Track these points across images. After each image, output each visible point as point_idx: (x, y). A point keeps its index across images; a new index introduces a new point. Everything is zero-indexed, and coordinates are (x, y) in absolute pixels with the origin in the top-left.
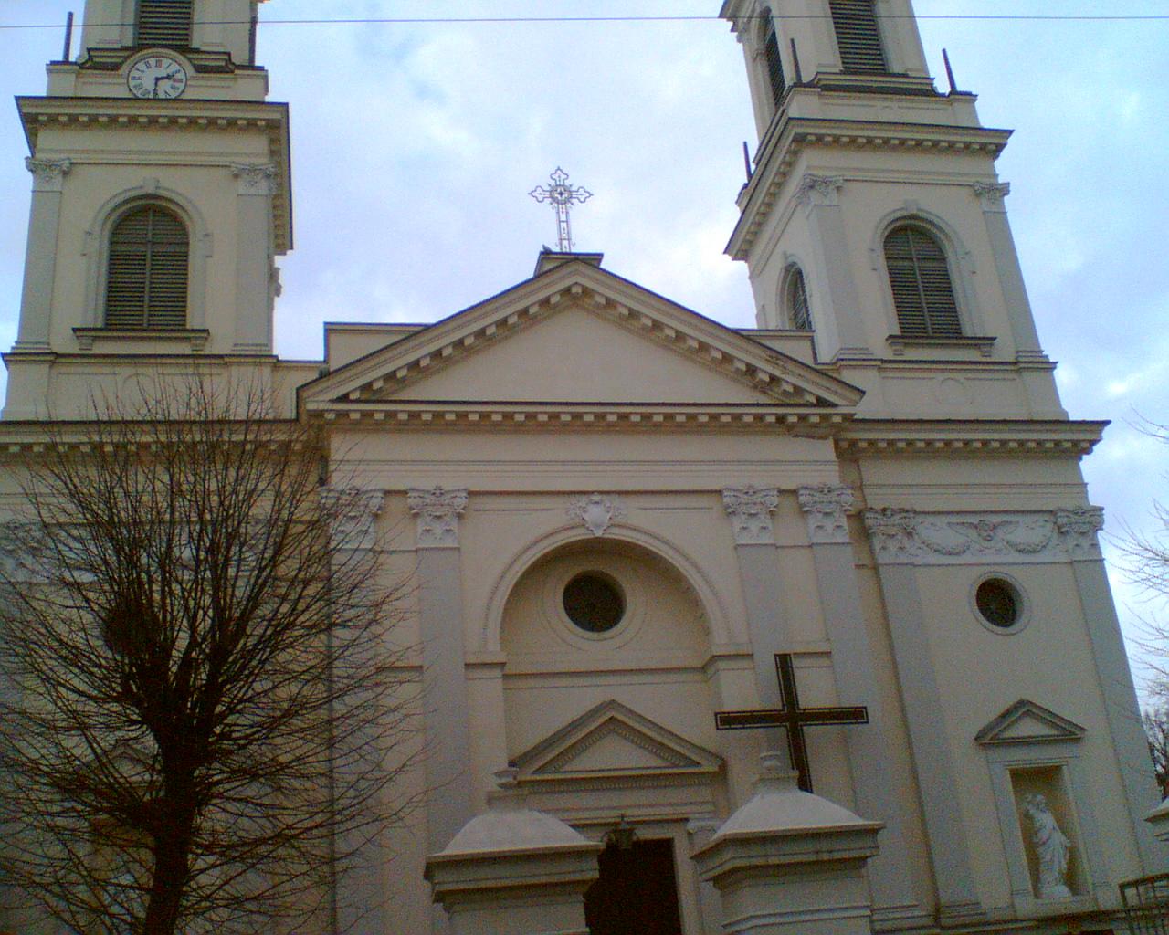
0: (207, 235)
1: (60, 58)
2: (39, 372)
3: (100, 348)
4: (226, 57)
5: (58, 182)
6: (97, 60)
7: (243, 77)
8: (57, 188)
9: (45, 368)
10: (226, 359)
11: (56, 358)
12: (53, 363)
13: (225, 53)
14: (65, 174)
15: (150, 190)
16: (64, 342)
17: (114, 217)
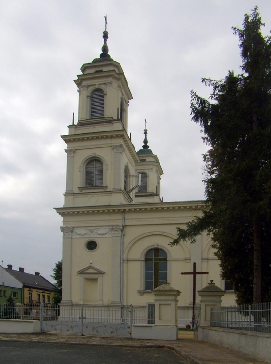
0: (106, 165)
1: (72, 124)
2: (71, 197)
3: (84, 191)
4: (112, 118)
5: (72, 154)
6: (81, 123)
7: (114, 123)
8: (72, 156)
9: (72, 196)
10: (111, 192)
11: (74, 194)
12: (73, 196)
13: (111, 117)
14: (74, 152)
15: (94, 155)
16: (76, 190)
17: (86, 162)
